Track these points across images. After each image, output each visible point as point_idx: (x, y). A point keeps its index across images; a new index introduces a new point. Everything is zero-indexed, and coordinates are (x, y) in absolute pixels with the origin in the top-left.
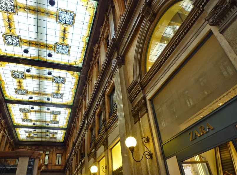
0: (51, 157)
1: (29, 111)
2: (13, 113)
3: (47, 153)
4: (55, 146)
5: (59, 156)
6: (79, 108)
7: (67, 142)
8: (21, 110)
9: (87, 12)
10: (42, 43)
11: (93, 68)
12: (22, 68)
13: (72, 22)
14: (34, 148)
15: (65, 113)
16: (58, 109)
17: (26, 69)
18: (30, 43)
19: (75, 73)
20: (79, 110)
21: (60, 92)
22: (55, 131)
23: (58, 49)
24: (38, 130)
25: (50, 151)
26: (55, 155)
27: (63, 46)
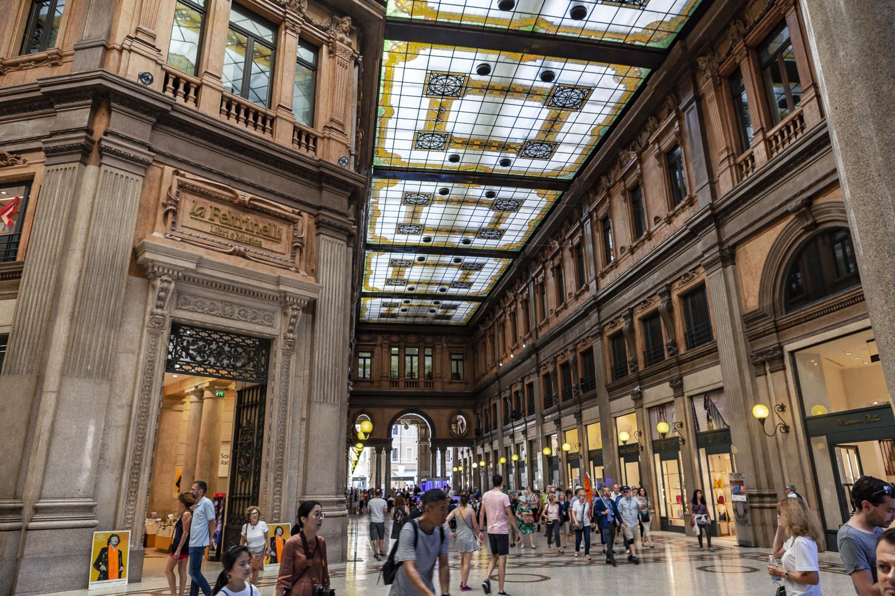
0: (438, 362)
1: (410, 264)
2: (373, 268)
3: (428, 351)
4: (446, 335)
5: (457, 360)
6: (544, 263)
7: (482, 329)
8: (392, 263)
9: (621, 87)
10: (495, 142)
11: (609, 195)
12: (429, 188)
13: (578, 106)
14: (395, 339)
15: (494, 266)
16: (480, 260)
17: (438, 188)
18: (467, 143)
19: (550, 192)
20: (544, 268)
21: (502, 226)
22: (455, 303)
23: (527, 152)
24: (414, 302)
25: (434, 349)
26: (446, 356)
27: (544, 145)
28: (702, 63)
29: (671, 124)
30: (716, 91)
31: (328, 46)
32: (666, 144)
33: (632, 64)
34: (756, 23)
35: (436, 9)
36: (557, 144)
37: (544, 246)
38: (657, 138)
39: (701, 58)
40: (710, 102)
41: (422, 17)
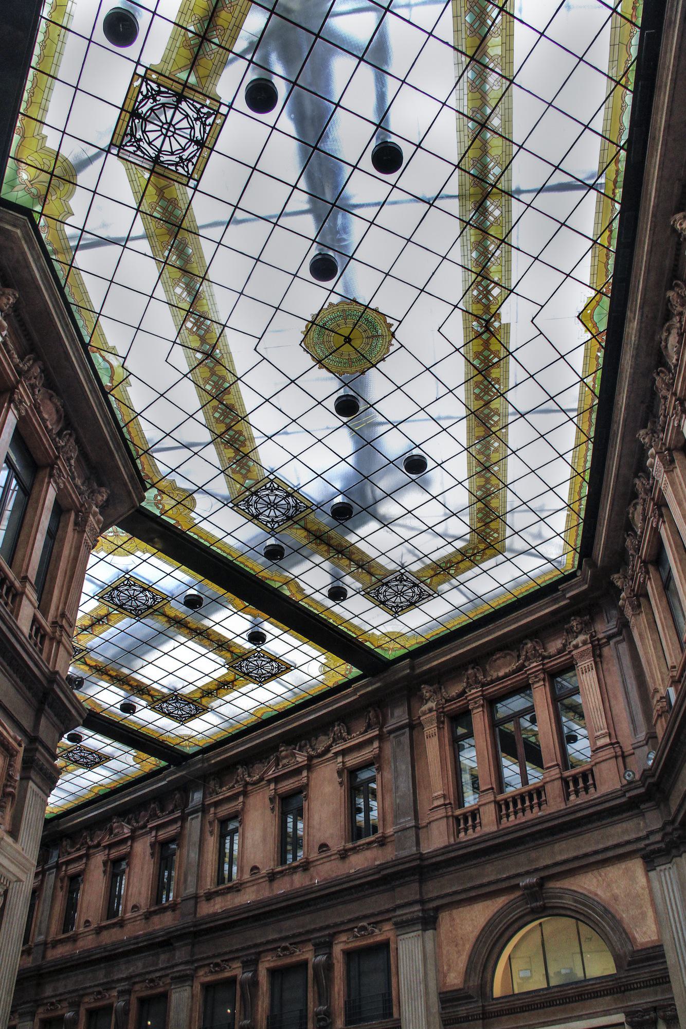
6: (89, 848)
11: (245, 793)
28: (426, 691)
29: (369, 742)
30: (439, 728)
31: (77, 516)
32: (353, 760)
33: (348, 660)
34: (499, 679)
35: (196, 521)
36: (205, 710)
37: (101, 823)
38: (343, 750)
39: (427, 687)
40: (429, 737)
41: (172, 522)
